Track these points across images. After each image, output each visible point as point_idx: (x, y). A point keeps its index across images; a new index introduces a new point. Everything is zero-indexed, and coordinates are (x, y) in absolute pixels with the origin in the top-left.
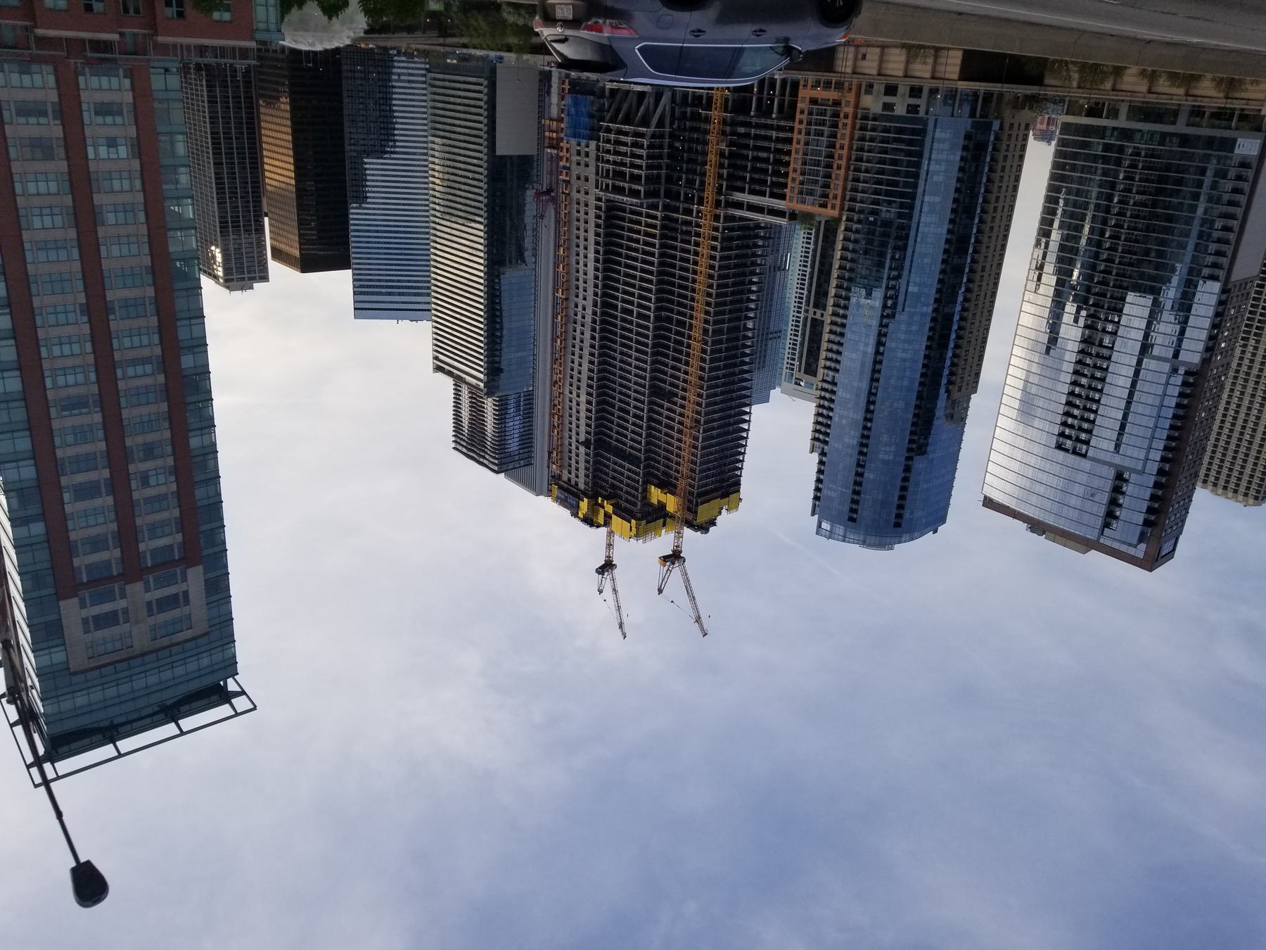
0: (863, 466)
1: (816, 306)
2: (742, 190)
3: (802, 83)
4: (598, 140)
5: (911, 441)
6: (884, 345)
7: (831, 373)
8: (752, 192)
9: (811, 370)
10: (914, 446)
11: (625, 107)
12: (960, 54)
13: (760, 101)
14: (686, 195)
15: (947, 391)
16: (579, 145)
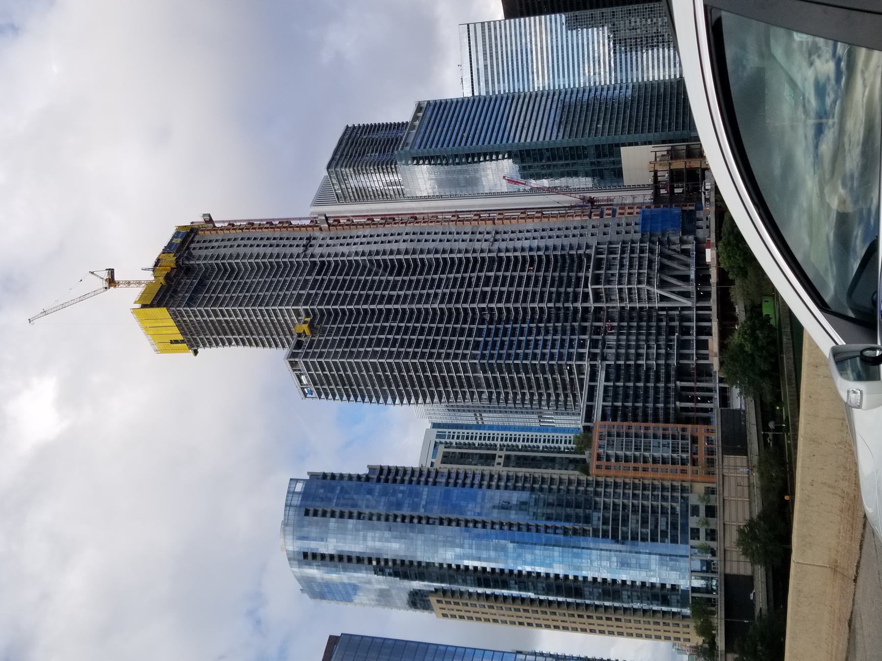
0: (359, 518)
1: (508, 458)
2: (607, 379)
3: (710, 427)
4: (642, 241)
5: (386, 561)
6: (475, 526)
7: (444, 480)
8: (606, 387)
9: (447, 458)
10: (382, 563)
11: (674, 265)
12: (749, 573)
13: (691, 389)
14: (599, 327)
15: (436, 590)
16: (636, 224)
